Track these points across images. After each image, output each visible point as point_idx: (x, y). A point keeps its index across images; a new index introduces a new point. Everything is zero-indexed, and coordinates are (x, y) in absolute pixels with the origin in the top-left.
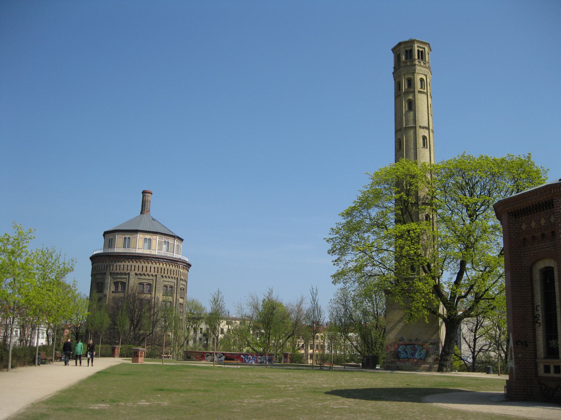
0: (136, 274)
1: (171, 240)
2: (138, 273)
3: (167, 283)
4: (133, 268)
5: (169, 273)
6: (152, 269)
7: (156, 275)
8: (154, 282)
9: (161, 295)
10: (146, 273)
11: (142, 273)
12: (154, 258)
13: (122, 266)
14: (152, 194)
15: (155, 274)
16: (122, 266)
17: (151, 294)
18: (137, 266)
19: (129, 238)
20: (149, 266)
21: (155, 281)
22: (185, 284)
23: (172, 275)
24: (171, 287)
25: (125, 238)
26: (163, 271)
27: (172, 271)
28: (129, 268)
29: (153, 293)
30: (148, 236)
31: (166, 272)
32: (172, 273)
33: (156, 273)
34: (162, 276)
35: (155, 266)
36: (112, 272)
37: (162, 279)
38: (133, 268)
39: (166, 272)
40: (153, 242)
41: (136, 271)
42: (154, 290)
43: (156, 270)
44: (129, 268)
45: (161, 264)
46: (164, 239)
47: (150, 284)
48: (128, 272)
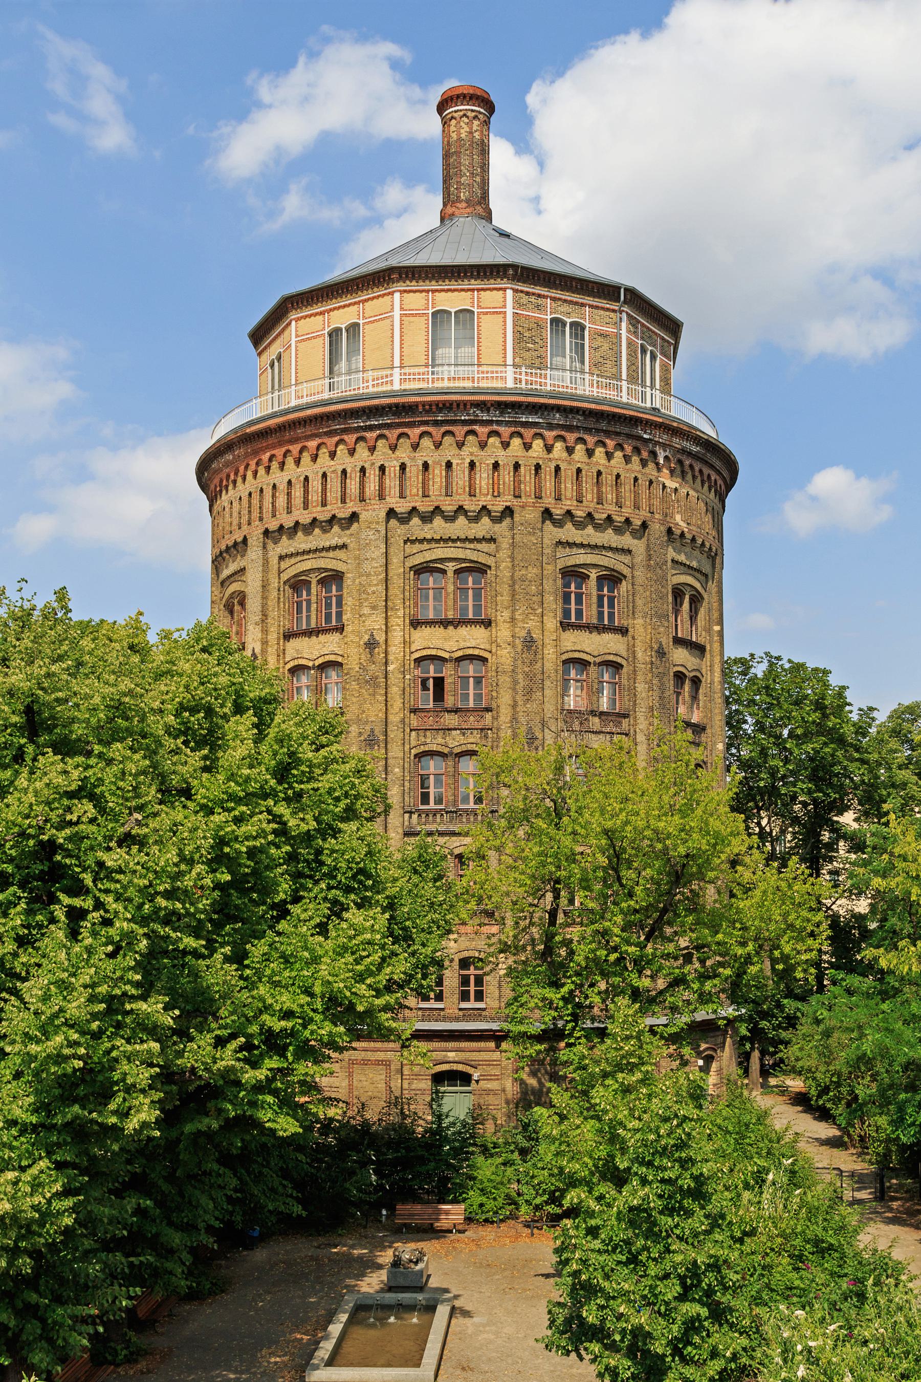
0: (391, 513)
1: (594, 318)
2: (402, 507)
3: (581, 557)
4: (372, 486)
5: (590, 496)
6: (483, 478)
7: (508, 512)
8: (504, 554)
9: (551, 623)
10: (449, 506)
11: (425, 507)
12: (482, 406)
13: (316, 484)
14: (490, 107)
15: (498, 506)
16: (316, 484)
17: (487, 624)
18: (393, 467)
19: (354, 328)
20: (460, 460)
21: (505, 543)
22: (707, 569)
23: (611, 509)
24: (612, 579)
25: (335, 334)
26: (548, 484)
27: (608, 479)
28: (353, 486)
29: (502, 617)
30: (452, 299)
31: (568, 488)
32: (610, 496)
33: (507, 500)
34: (547, 514)
35: (502, 456)
36: (273, 525)
37: (552, 533)
38: (372, 486)
39: (568, 488)
40: (488, 326)
41: (392, 501)
42: (504, 598)
43: (507, 476)
44: (353, 486)
45: (538, 444)
46: (551, 307)
47: (480, 569)
48: (352, 506)
